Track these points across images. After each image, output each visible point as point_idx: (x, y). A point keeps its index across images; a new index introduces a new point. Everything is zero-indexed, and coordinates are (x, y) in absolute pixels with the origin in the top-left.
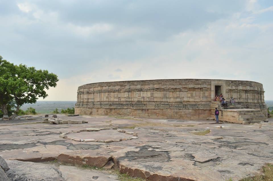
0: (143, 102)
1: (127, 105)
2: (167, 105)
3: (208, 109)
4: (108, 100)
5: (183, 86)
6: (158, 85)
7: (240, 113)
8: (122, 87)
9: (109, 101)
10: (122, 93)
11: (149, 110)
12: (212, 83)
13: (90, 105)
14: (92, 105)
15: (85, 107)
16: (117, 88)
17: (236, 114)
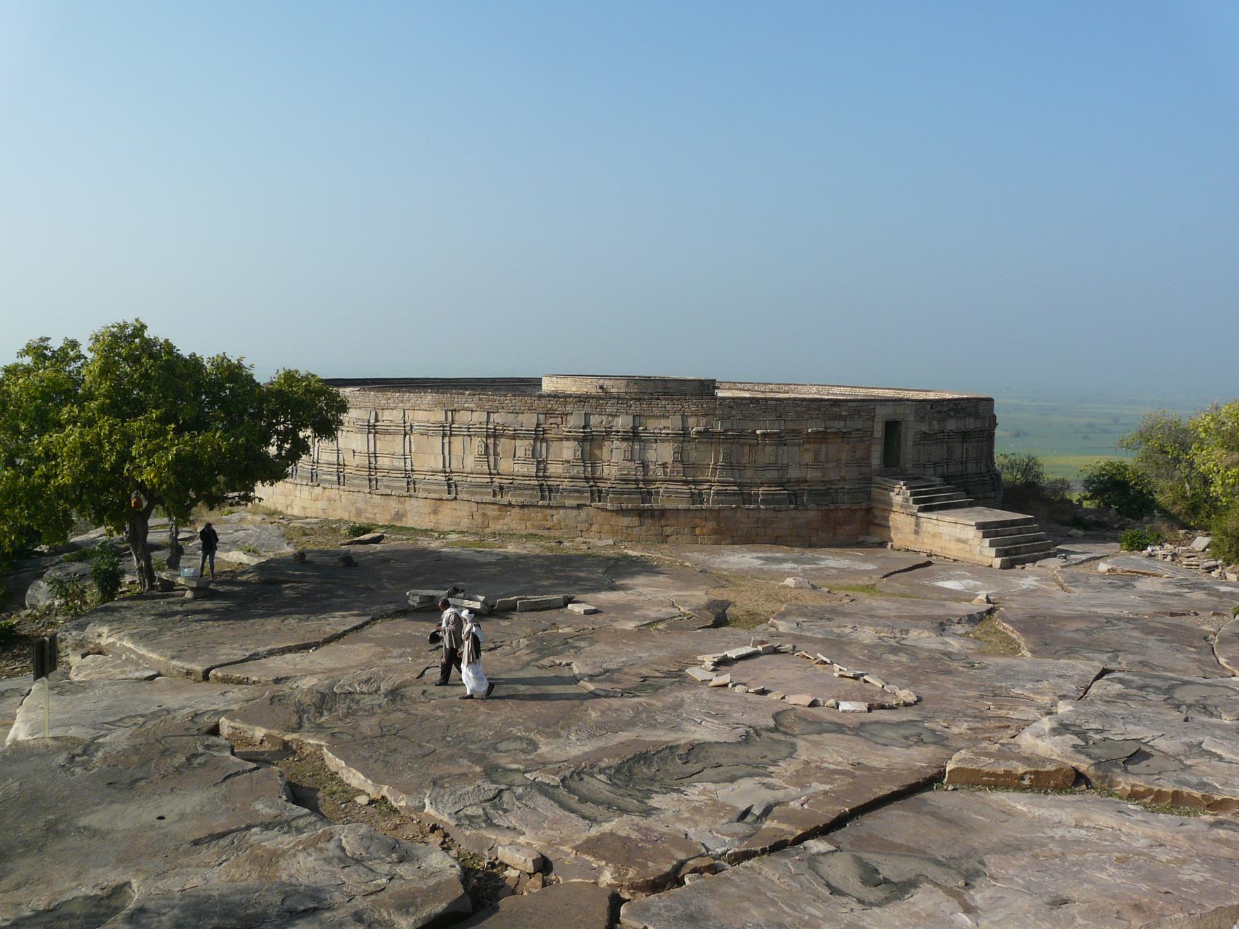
1: (578, 491)
3: (863, 506)
5: (791, 426)
7: (987, 529)
8: (551, 420)
11: (668, 514)
12: (877, 412)
17: (972, 534)
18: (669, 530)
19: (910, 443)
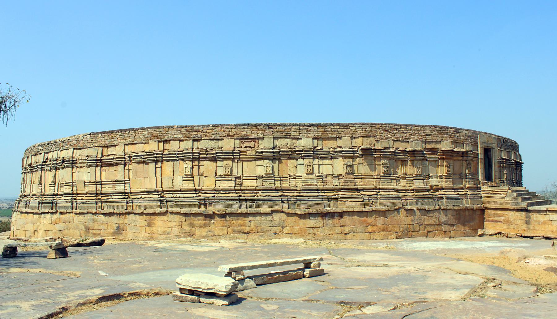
0: (323, 190)
2: (395, 198)
4: (190, 185)
6: (365, 139)
9: (198, 188)
10: (245, 163)
13: (114, 204)
14: (125, 204)
15: (87, 213)
16: (228, 145)
18: (347, 229)
19: (497, 165)
